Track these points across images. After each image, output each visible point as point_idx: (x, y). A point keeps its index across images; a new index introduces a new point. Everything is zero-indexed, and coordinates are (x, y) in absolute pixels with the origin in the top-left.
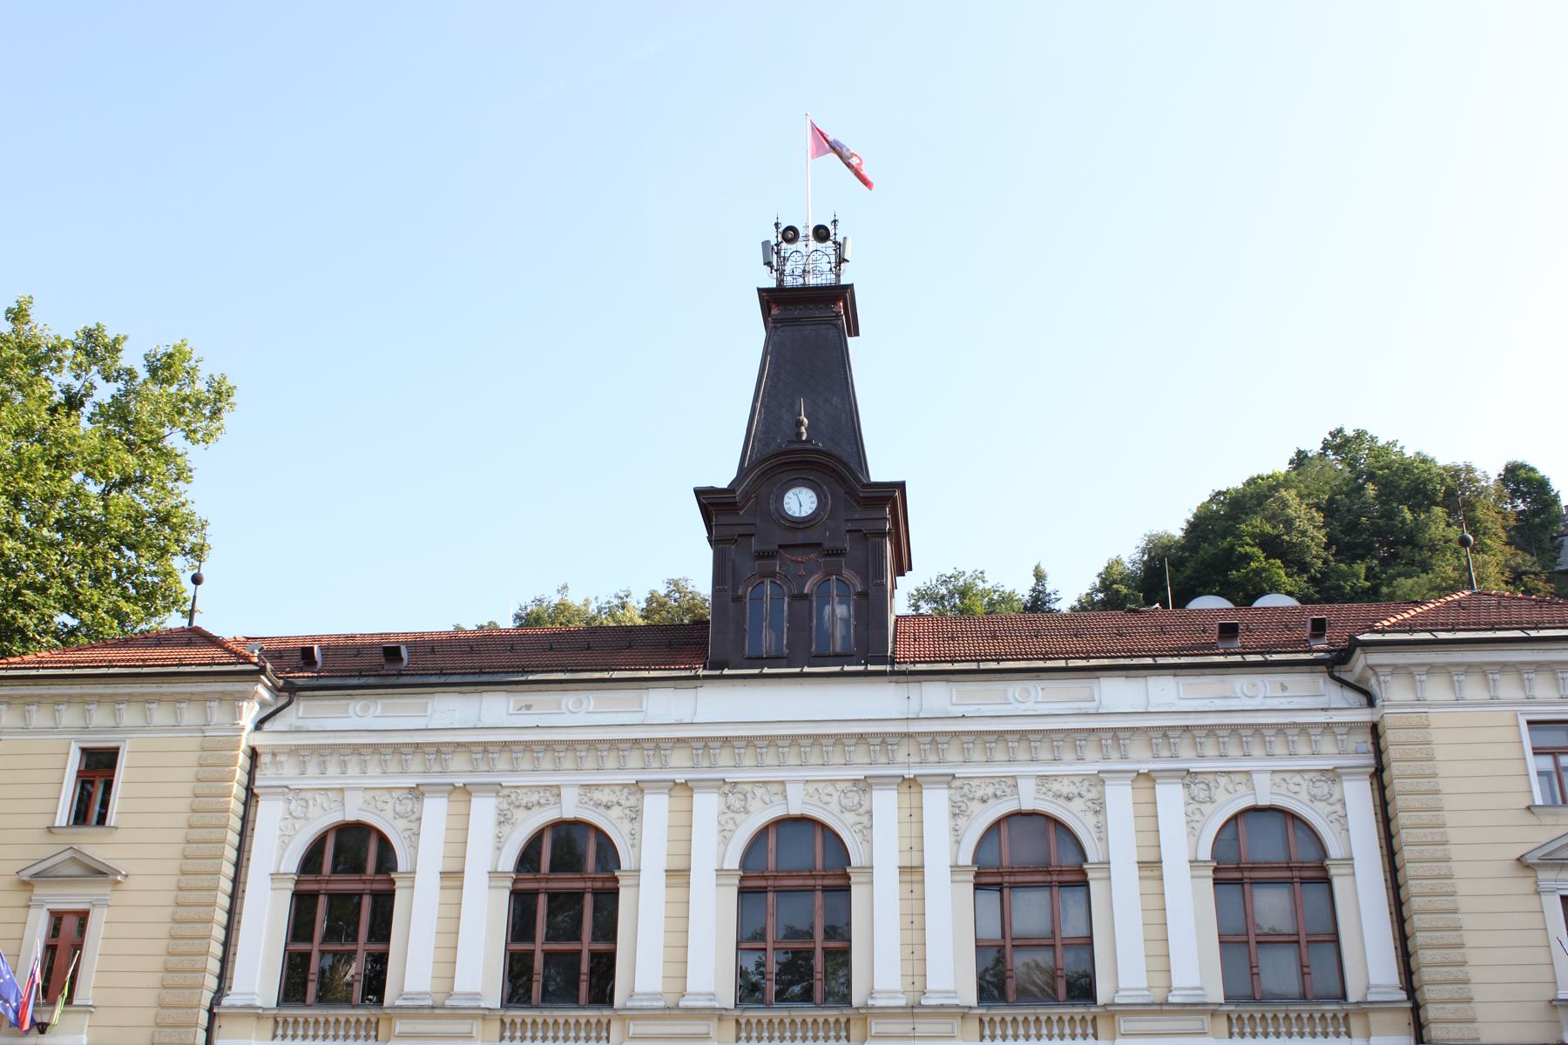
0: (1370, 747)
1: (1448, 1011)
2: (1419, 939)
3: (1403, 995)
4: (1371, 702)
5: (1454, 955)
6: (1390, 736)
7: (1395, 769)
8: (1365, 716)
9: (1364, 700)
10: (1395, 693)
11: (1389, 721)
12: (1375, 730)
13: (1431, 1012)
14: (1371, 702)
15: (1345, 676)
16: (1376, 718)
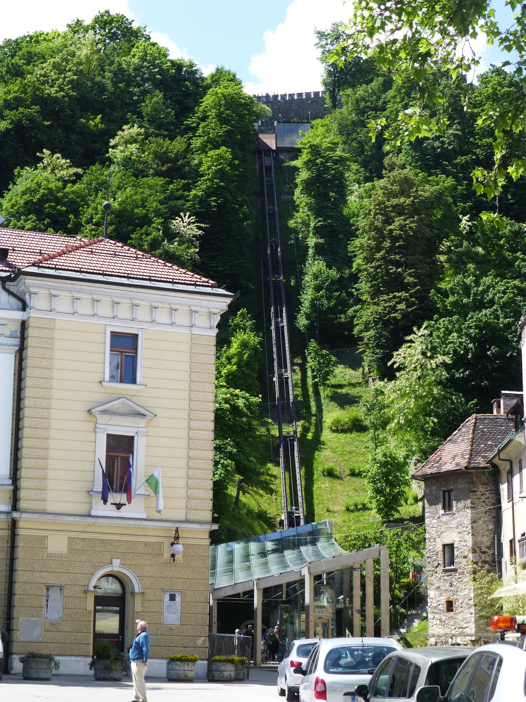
0: (19, 334)
1: (32, 494)
2: (24, 452)
3: (10, 482)
4: (24, 307)
5: (42, 463)
6: (31, 332)
7: (30, 352)
8: (19, 315)
9: (20, 304)
10: (38, 303)
11: (31, 323)
12: (24, 325)
13: (22, 494)
14: (24, 307)
15: (13, 289)
16: (25, 318)
